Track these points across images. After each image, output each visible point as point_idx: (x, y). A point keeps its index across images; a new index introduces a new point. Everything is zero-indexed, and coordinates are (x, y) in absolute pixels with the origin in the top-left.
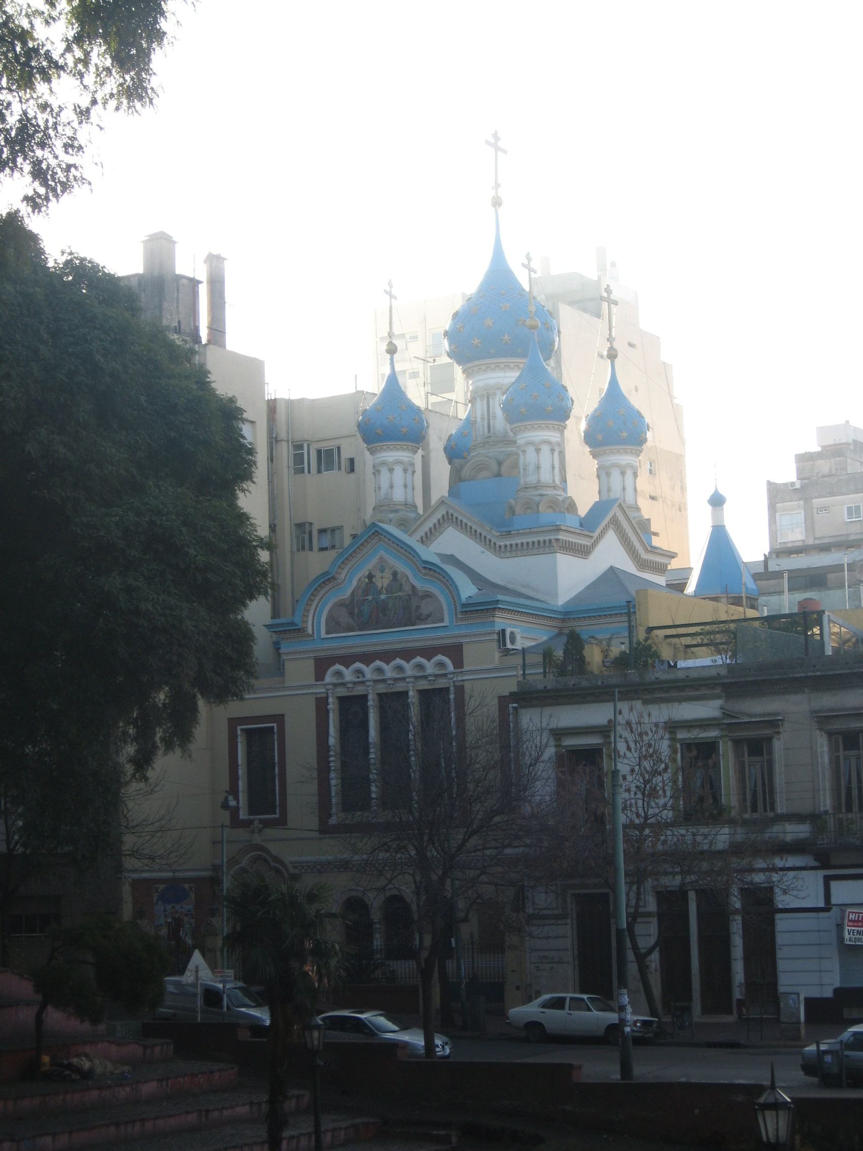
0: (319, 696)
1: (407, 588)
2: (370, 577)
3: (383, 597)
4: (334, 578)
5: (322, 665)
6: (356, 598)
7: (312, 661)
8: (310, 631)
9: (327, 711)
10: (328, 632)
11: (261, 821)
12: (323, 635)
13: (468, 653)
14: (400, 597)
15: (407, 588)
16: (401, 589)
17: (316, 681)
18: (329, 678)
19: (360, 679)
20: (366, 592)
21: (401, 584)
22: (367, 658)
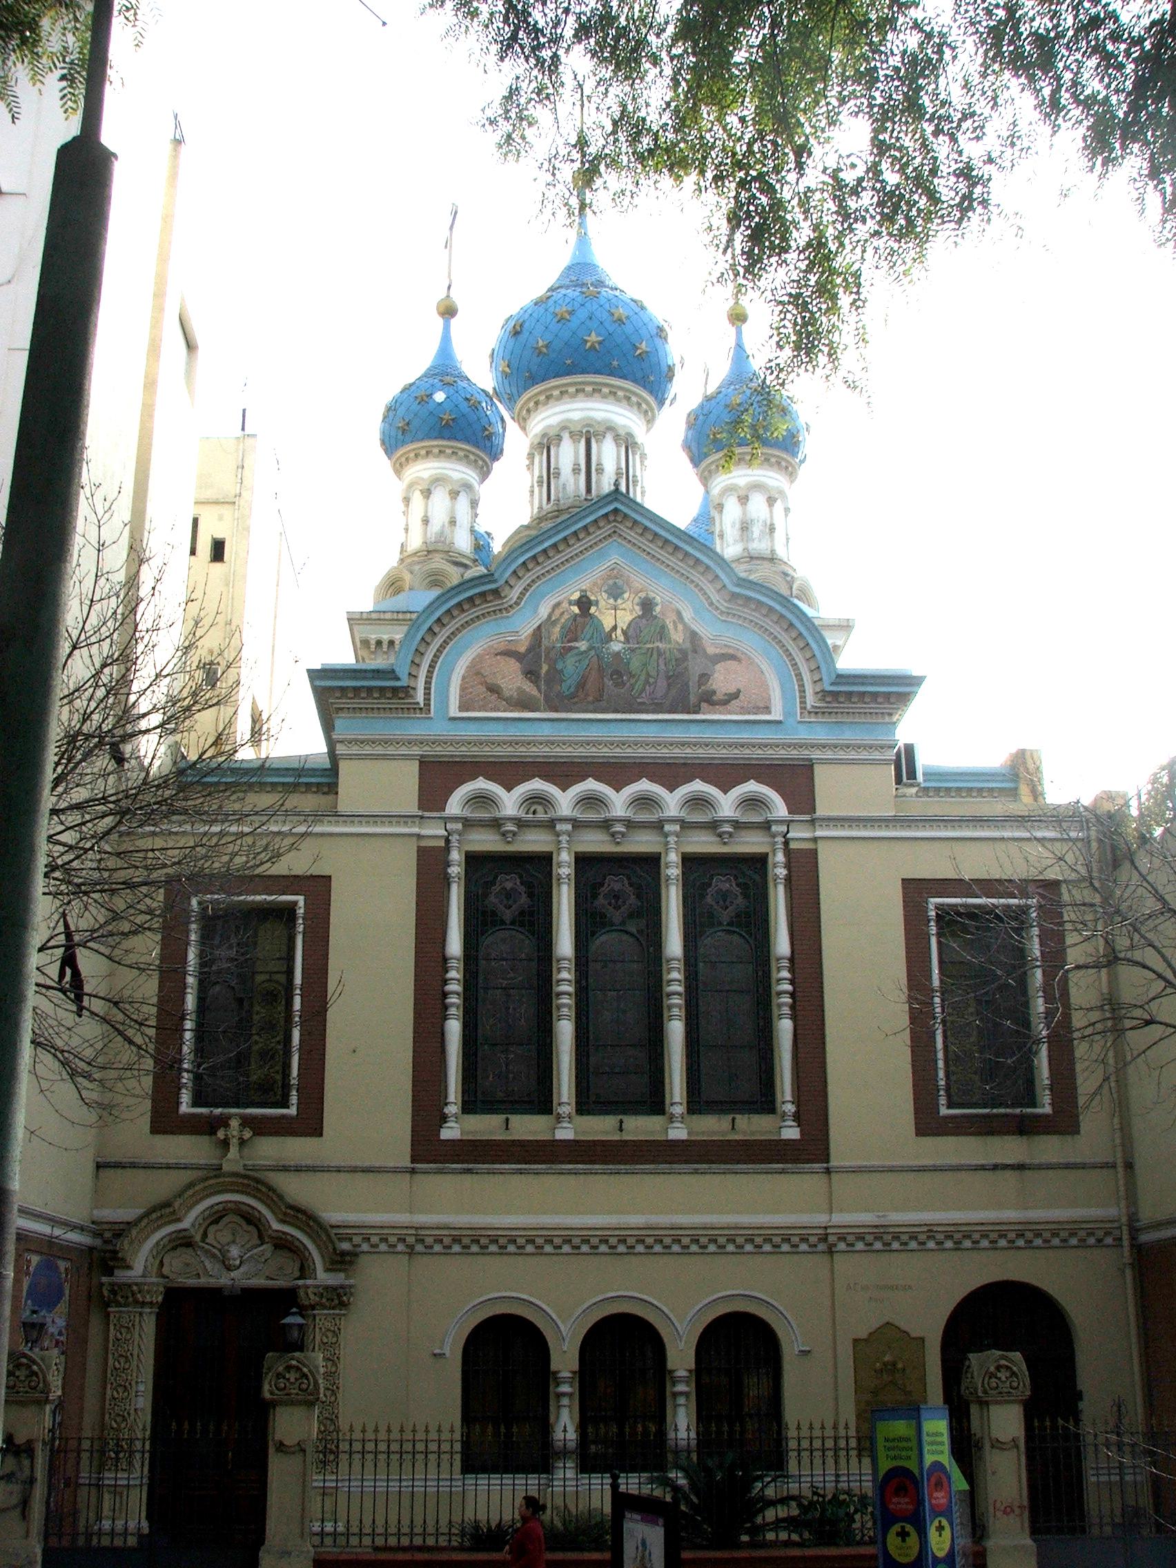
0: (424, 843)
1: (677, 636)
2: (584, 603)
3: (616, 647)
4: (496, 593)
5: (438, 776)
6: (545, 642)
7: (414, 767)
8: (420, 697)
9: (446, 881)
10: (461, 709)
11: (246, 1122)
12: (454, 711)
13: (824, 778)
14: (660, 653)
15: (677, 636)
16: (662, 633)
17: (421, 806)
18: (455, 805)
19: (541, 815)
20: (572, 632)
21: (663, 627)
22: (564, 772)
